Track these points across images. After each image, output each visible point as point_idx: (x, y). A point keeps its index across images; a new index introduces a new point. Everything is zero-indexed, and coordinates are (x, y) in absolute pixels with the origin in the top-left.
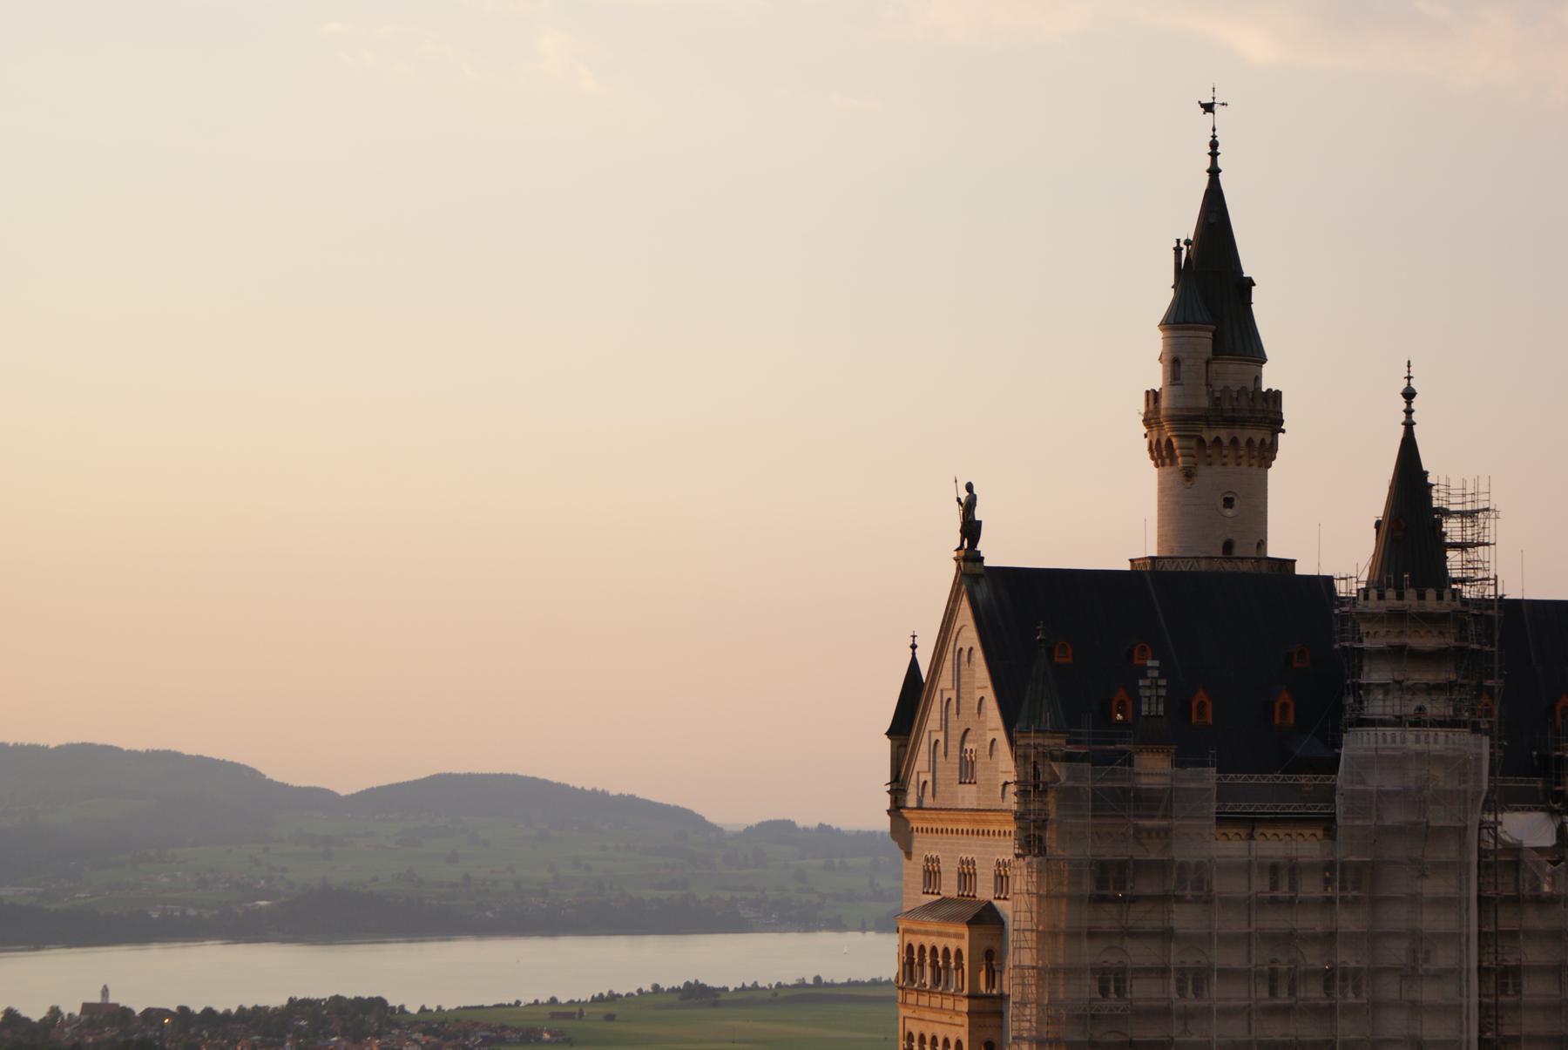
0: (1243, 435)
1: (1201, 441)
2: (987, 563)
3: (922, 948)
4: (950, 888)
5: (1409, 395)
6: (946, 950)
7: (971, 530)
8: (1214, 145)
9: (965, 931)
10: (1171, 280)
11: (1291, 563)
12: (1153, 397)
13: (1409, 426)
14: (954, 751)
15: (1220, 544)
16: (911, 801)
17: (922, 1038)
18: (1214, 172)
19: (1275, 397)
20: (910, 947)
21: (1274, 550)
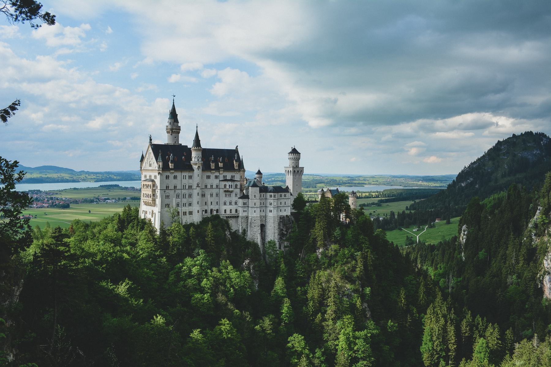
0: (177, 131)
1: (173, 131)
2: (153, 143)
3: (145, 184)
4: (148, 178)
5: (197, 127)
6: (149, 185)
7: (151, 140)
8: (174, 100)
9: (151, 182)
10: (169, 114)
11: (181, 144)
12: (167, 126)
13: (197, 130)
14: (149, 164)
15: (174, 142)
16: (143, 169)
17: (145, 194)
18: (174, 103)
19: (180, 127)
20: (144, 184)
21: (179, 143)
